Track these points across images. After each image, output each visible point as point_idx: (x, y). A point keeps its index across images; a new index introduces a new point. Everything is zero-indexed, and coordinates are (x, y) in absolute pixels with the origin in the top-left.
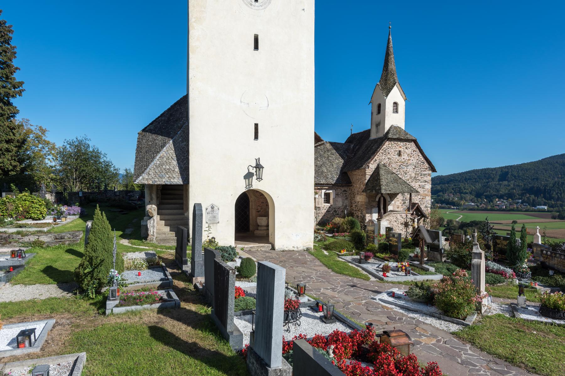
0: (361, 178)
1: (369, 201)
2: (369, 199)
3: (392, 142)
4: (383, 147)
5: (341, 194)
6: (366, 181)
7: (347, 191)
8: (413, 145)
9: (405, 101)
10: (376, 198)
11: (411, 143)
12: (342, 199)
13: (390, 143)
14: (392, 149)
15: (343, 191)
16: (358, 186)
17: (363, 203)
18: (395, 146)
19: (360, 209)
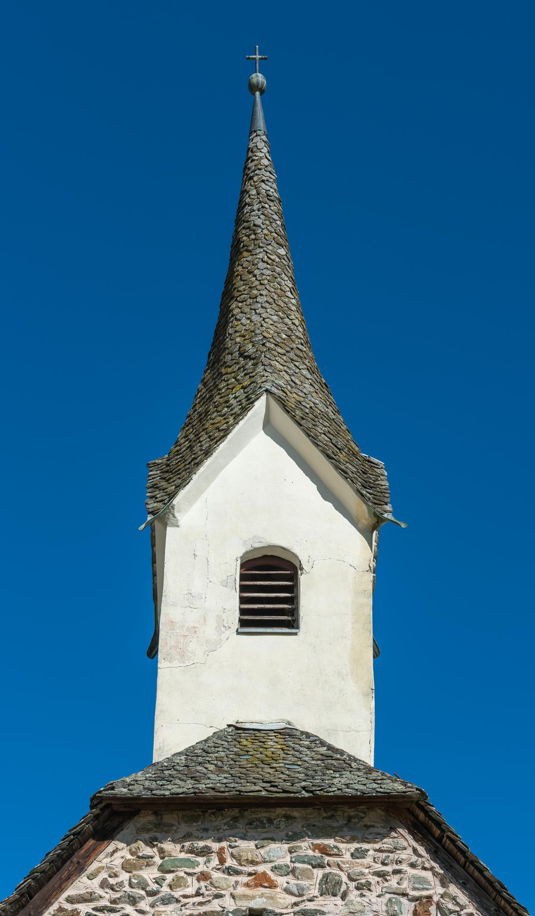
3: (168, 846)
4: (71, 891)
8: (406, 855)
9: (367, 533)
11: (387, 843)
13: (147, 851)
14: (167, 901)
18: (204, 877)
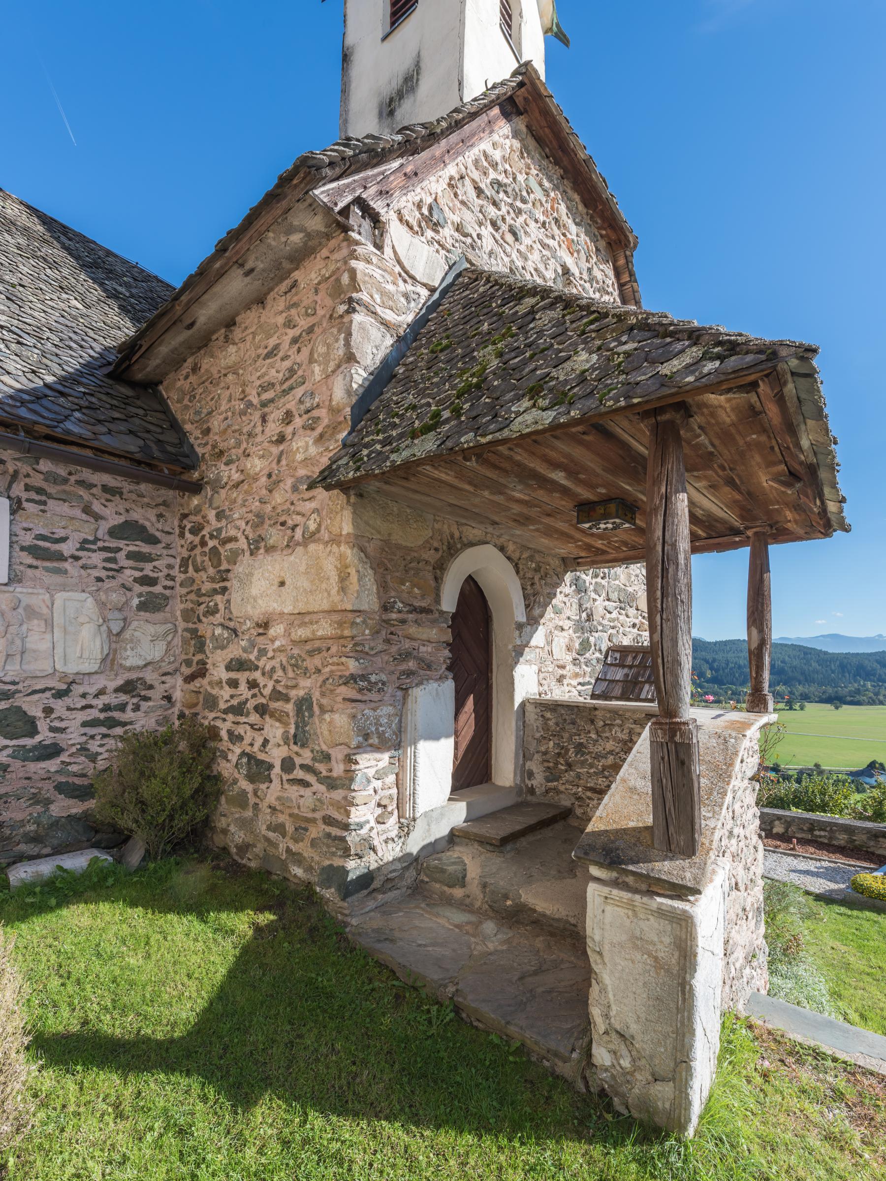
0: (292, 371)
1: (386, 608)
2: (383, 586)
5: (97, 558)
6: (359, 376)
7: (153, 540)
10: (438, 580)
12: (102, 605)
15: (115, 532)
16: (256, 465)
17: (325, 629)
19: (277, 695)
